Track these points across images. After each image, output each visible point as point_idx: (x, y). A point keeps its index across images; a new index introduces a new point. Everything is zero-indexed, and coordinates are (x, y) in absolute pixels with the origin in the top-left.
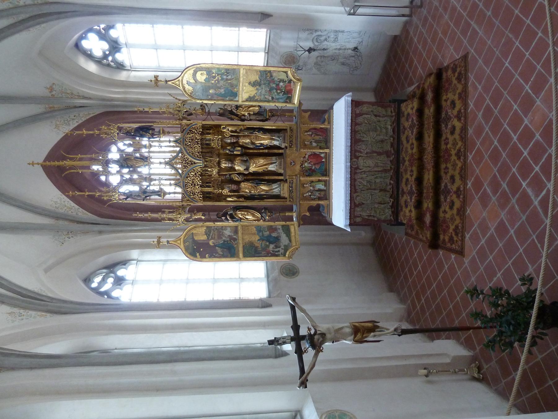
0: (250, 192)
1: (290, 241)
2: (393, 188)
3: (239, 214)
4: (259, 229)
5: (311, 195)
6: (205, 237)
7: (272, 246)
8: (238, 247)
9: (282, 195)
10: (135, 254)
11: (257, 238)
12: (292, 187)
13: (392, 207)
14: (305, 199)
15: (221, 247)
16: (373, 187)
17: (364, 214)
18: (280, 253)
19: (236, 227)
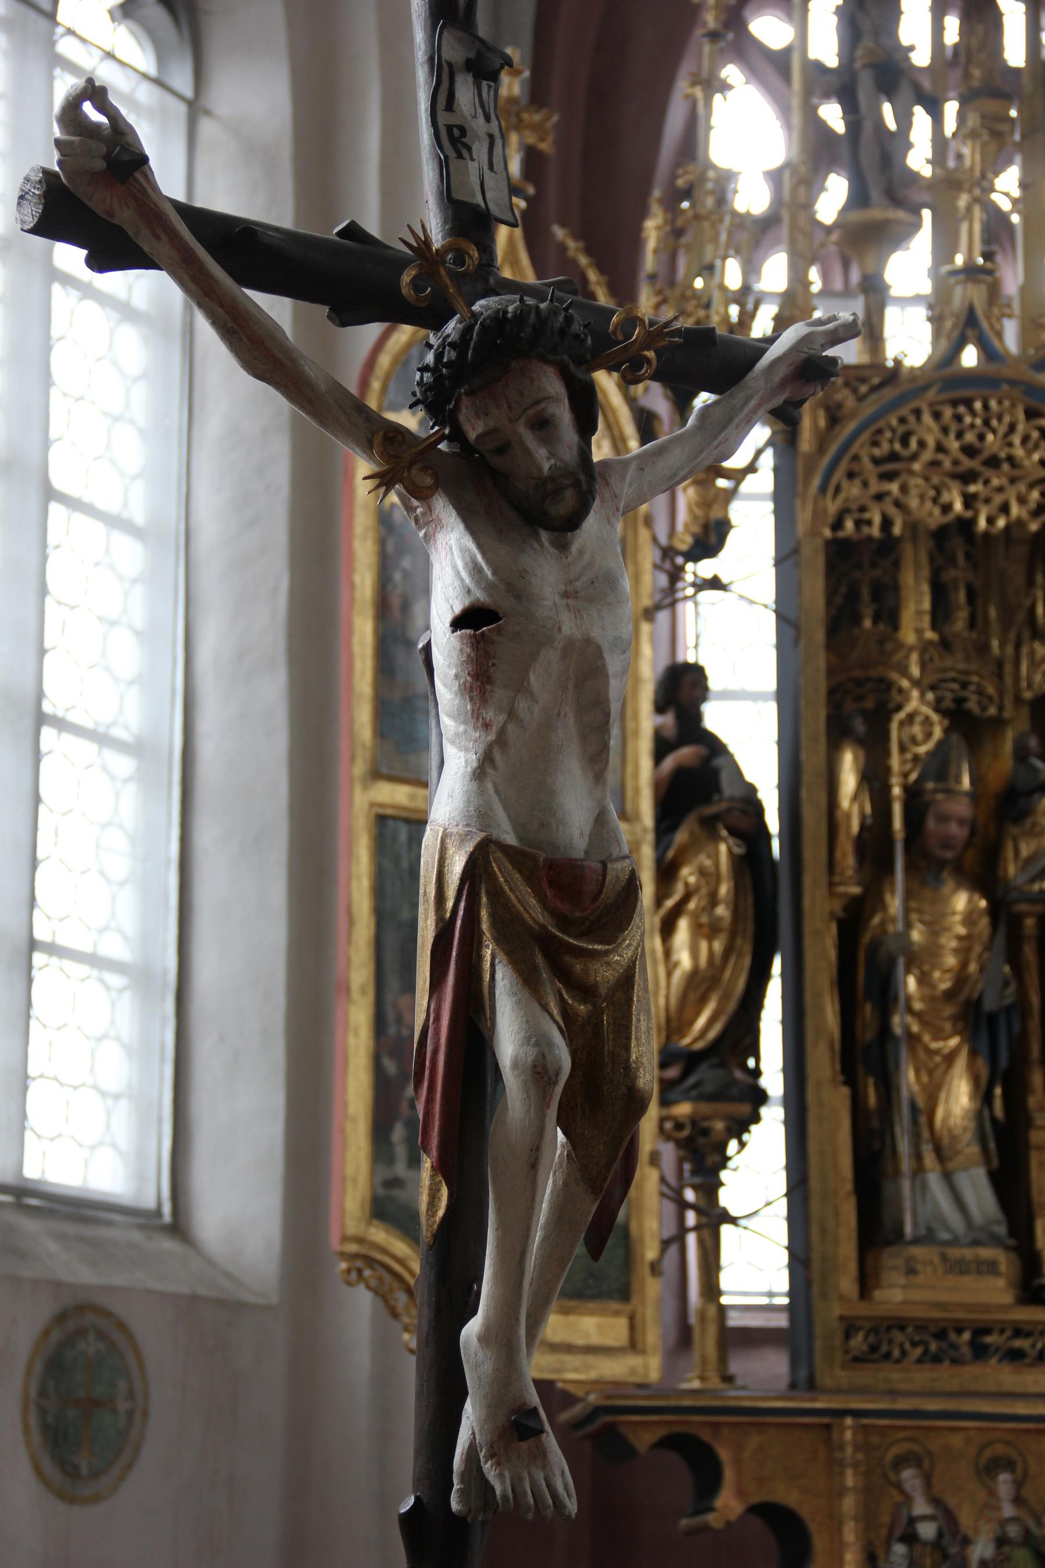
0: (914, 959)
5: (910, 1538)
9: (892, 1259)
12: (980, 1352)
14: (879, 1482)
18: (400, 1169)
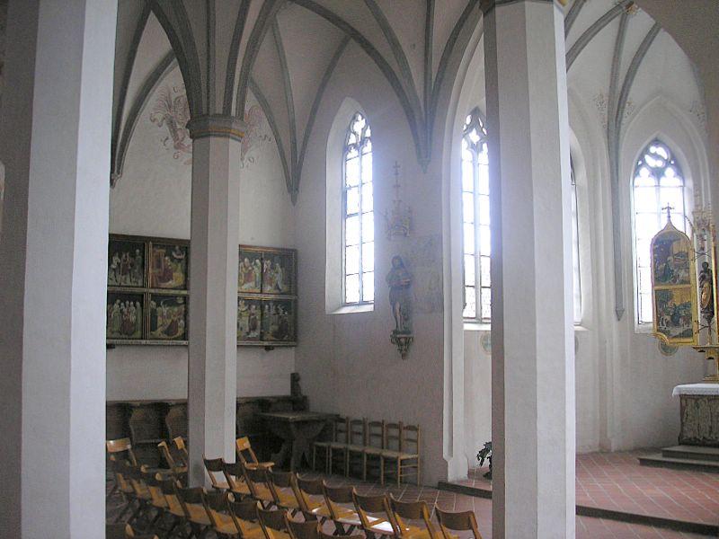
1: (675, 337)
2: (713, 440)
3: (706, 285)
4: (687, 306)
6: (676, 251)
7: (668, 318)
8: (666, 285)
10: (690, 183)
11: (678, 304)
13: (695, 438)
15: (665, 268)
16: (715, 419)
17: (688, 409)
19: (689, 282)
